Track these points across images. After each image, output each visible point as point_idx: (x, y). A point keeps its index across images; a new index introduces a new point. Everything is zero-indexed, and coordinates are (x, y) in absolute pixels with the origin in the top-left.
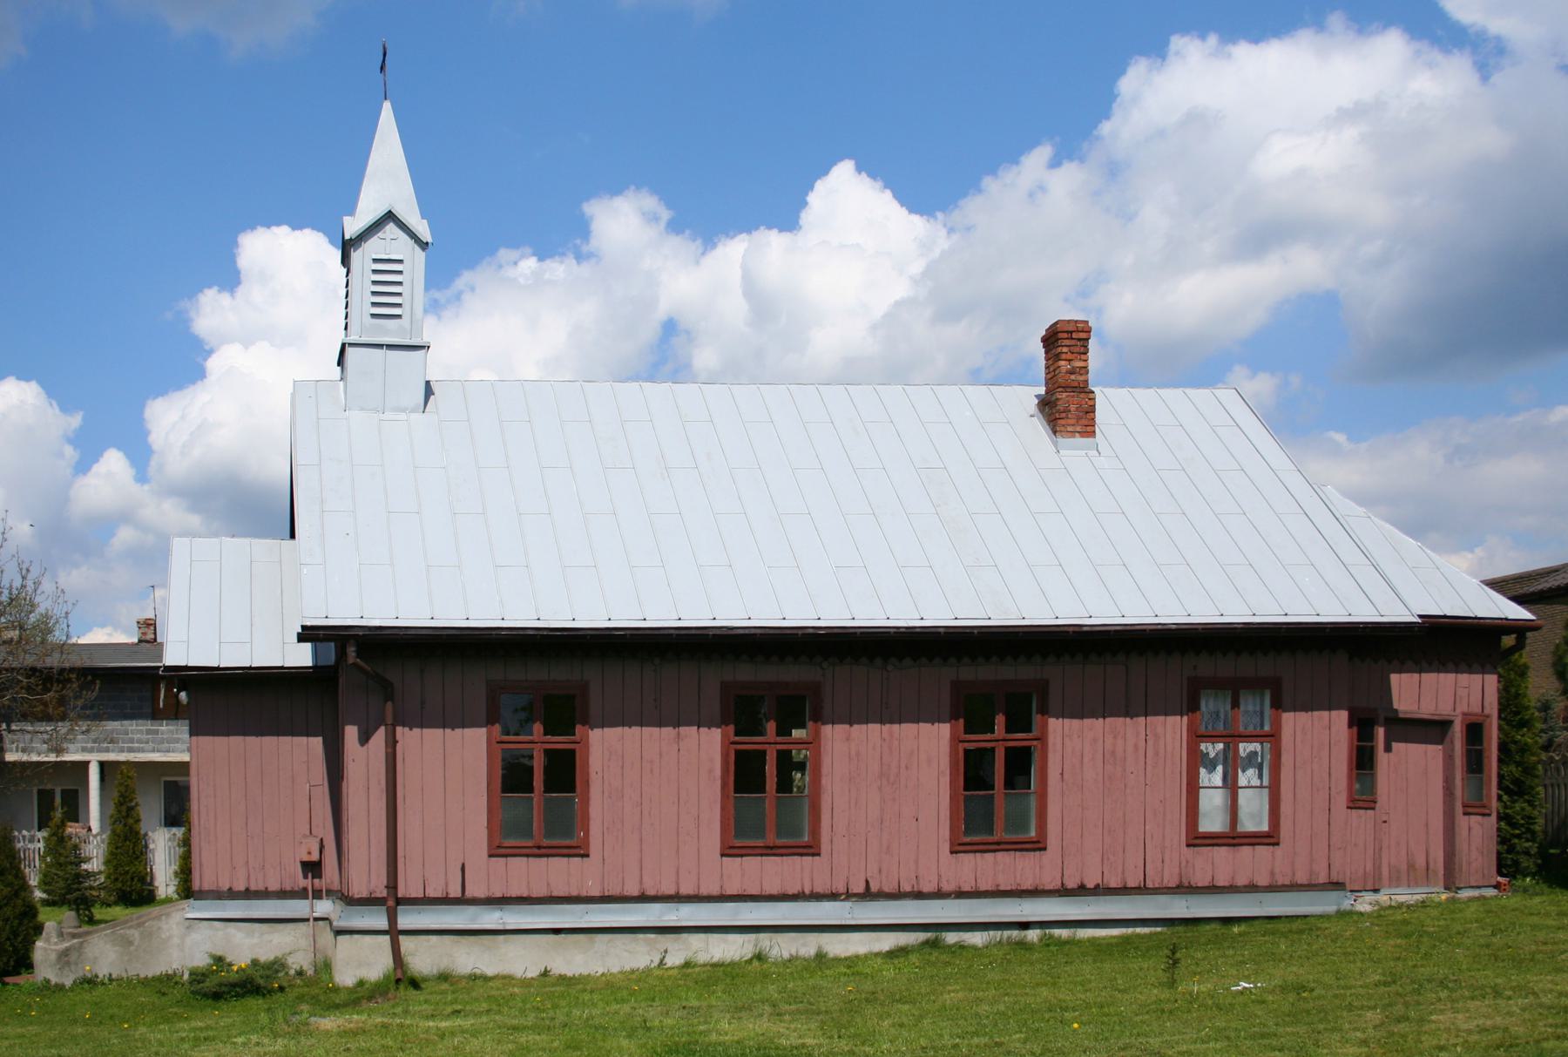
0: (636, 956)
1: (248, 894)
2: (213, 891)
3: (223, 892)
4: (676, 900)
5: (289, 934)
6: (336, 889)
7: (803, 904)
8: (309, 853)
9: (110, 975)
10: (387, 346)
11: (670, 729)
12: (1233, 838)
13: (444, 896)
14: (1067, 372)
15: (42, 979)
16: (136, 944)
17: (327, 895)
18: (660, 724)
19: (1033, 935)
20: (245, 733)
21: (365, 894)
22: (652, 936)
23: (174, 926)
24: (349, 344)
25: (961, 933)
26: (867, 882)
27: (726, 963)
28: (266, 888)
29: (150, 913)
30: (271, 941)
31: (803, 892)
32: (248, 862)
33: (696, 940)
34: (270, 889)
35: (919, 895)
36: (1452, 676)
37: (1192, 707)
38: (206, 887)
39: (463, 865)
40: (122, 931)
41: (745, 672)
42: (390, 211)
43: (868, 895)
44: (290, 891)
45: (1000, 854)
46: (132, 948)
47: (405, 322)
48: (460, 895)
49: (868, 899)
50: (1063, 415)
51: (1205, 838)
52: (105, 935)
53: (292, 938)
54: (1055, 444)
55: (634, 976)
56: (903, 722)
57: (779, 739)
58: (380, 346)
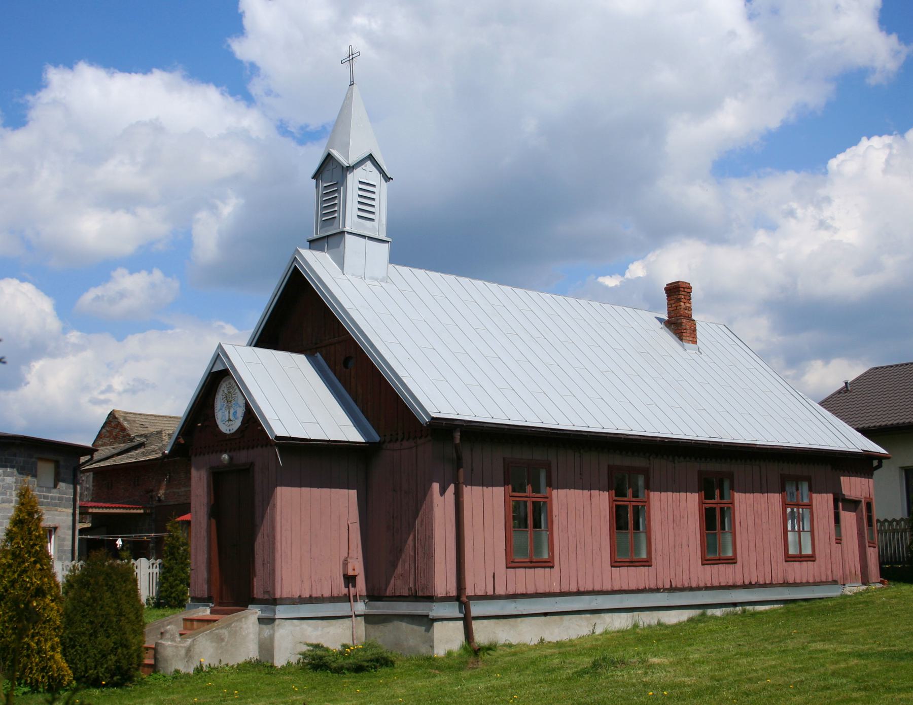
0: (621, 622)
1: (312, 600)
2: (289, 598)
3: (295, 599)
4: (593, 594)
5: (340, 627)
6: (364, 595)
7: (647, 594)
8: (354, 570)
9: (210, 665)
10: (368, 237)
11: (587, 491)
12: (800, 558)
13: (485, 594)
14: (684, 309)
15: (173, 670)
16: (226, 640)
17: (360, 599)
18: (583, 489)
19: (739, 609)
20: (311, 486)
21: (444, 594)
22: (589, 615)
23: (251, 626)
24: (347, 232)
25: (712, 610)
26: (671, 581)
27: (624, 630)
28: (322, 595)
29: (240, 615)
30: (329, 632)
31: (646, 588)
32: (311, 577)
33: (607, 617)
34: (325, 596)
35: (691, 589)
36: (859, 478)
37: (782, 490)
38: (285, 596)
39: (494, 574)
40: (217, 631)
41: (619, 460)
42: (371, 154)
43: (672, 589)
44: (337, 597)
45: (720, 565)
46: (223, 644)
47: (376, 223)
48: (492, 594)
49: (672, 591)
50: (685, 331)
51: (791, 557)
52: (206, 634)
53: (341, 630)
54: (683, 347)
55: (549, 644)
56: (755, 493)
57: (634, 499)
58: (364, 237)
